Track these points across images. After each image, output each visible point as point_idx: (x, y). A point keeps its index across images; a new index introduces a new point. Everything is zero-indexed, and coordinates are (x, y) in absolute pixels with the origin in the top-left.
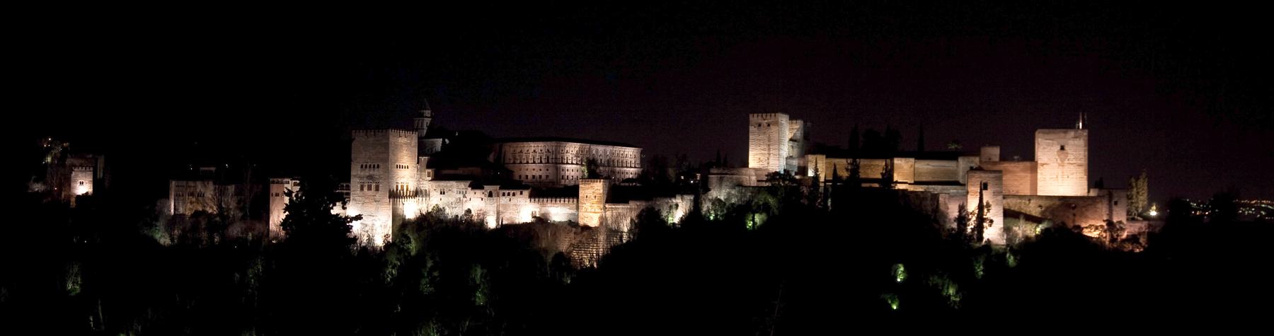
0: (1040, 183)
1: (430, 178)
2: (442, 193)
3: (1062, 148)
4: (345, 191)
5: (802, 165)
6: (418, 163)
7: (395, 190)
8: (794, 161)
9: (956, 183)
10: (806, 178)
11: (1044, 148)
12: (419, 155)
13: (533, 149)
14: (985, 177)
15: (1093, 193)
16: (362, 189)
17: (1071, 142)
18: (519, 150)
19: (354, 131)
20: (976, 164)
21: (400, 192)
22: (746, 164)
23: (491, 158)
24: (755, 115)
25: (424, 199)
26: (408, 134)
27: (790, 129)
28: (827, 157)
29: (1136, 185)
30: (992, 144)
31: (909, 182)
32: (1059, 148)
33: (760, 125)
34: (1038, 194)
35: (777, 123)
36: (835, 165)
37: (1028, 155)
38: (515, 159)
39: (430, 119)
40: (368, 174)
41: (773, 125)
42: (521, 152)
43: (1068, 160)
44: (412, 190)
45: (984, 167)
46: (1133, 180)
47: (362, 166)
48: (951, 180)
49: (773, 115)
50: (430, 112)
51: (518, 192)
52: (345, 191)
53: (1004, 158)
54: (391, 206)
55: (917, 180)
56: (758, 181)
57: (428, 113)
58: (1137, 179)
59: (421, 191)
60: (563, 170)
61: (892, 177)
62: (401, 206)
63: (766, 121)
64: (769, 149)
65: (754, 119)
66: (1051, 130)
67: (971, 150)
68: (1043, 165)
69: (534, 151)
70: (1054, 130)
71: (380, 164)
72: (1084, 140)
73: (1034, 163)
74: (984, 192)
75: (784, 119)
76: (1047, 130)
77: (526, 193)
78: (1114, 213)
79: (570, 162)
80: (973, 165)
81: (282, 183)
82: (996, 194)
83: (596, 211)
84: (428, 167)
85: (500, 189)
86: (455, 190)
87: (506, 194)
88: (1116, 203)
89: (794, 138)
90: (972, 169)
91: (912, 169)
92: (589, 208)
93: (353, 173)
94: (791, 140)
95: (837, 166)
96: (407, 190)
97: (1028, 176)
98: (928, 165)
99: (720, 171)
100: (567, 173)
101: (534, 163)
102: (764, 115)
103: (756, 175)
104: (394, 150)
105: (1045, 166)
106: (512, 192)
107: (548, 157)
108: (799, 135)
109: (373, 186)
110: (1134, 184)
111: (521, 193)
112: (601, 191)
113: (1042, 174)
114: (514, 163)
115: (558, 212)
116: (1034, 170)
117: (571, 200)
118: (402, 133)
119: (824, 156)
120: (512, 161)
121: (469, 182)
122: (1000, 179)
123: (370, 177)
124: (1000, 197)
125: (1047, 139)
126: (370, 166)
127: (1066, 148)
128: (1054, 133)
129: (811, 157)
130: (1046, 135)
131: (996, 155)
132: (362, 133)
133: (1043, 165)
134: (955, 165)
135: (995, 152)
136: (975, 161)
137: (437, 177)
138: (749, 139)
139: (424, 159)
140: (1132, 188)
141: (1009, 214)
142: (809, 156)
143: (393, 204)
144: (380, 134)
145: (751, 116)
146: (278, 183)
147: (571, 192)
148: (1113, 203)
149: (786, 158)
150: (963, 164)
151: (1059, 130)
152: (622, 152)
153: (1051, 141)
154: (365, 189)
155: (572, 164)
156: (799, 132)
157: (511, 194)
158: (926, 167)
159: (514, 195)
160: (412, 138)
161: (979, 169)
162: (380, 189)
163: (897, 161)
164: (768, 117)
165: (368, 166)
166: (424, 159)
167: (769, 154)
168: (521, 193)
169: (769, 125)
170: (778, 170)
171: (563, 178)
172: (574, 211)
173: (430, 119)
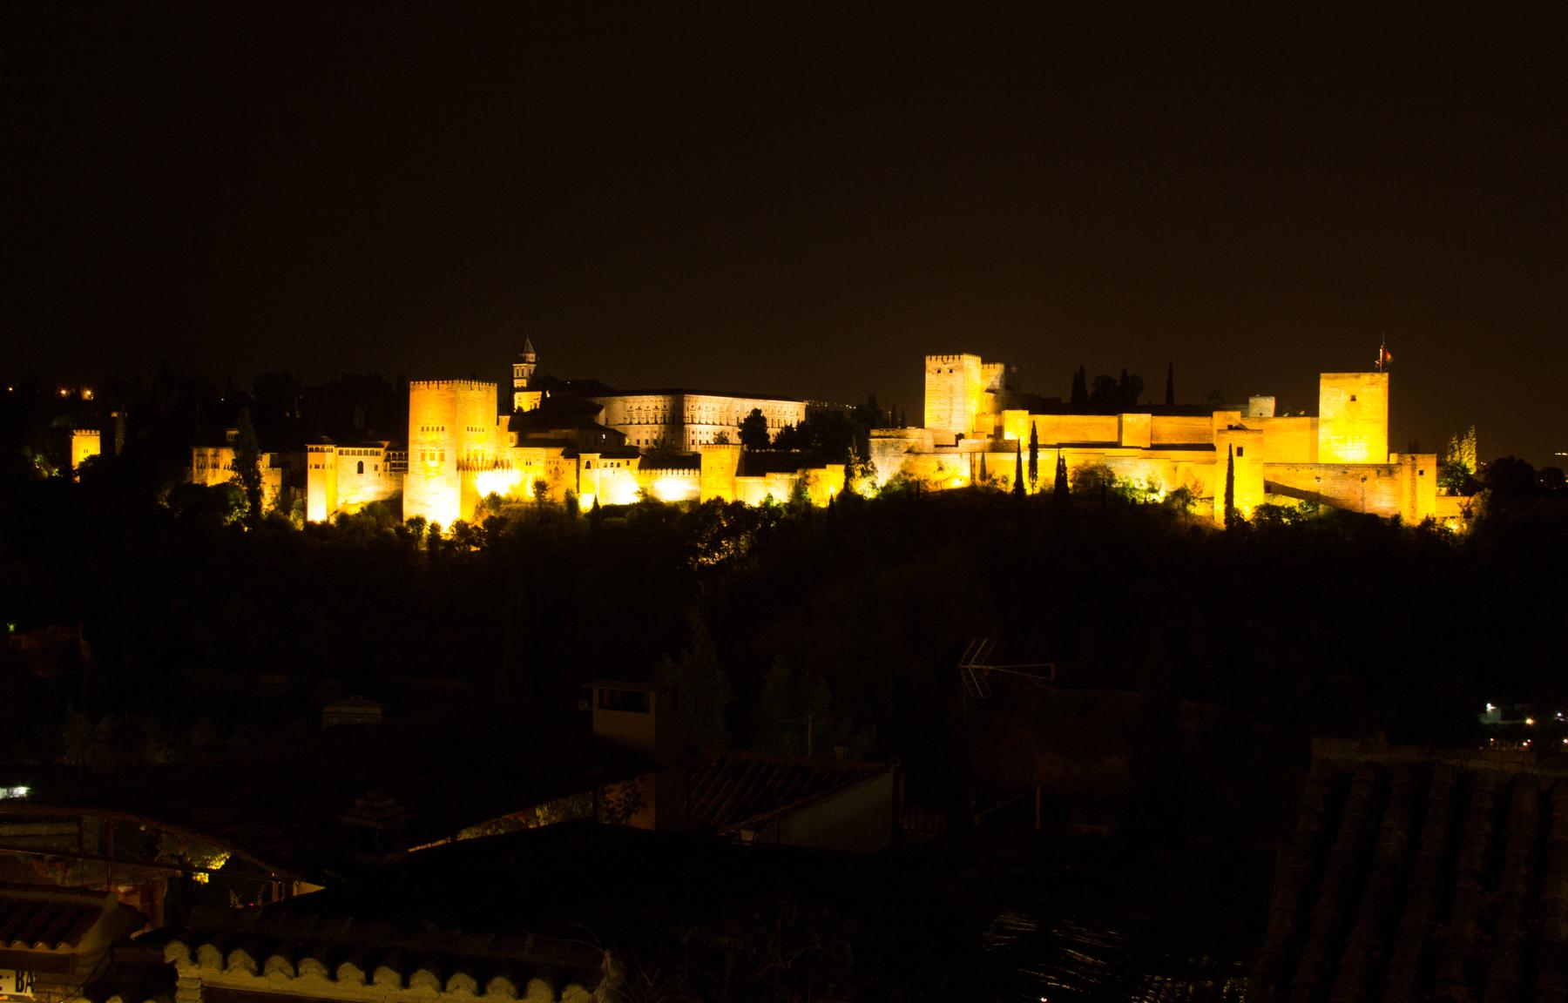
0: (1321, 447)
1: (514, 444)
2: (528, 463)
3: (1353, 399)
4: (404, 462)
5: (997, 425)
6: (498, 424)
7: (465, 460)
8: (987, 419)
9: (1211, 447)
10: (1000, 441)
11: (1328, 399)
12: (498, 415)
13: (652, 406)
14: (1237, 439)
15: (1394, 458)
16: (423, 457)
17: (1365, 390)
18: (636, 406)
19: (412, 383)
20: (1237, 421)
21: (472, 463)
22: (920, 424)
23: (602, 418)
24: (934, 358)
25: (505, 470)
26: (483, 386)
27: (982, 377)
28: (1030, 413)
29: (1460, 449)
30: (1265, 394)
31: (1143, 446)
32: (1348, 398)
33: (939, 372)
34: (1322, 460)
35: (961, 368)
36: (1034, 423)
37: (1309, 406)
38: (632, 418)
39: (534, 365)
40: (430, 439)
41: (956, 370)
42: (639, 408)
43: (1361, 414)
44: (489, 460)
45: (1247, 424)
46: (1455, 441)
47: (423, 430)
48: (1202, 442)
49: (956, 357)
50: (533, 355)
51: (623, 462)
52: (404, 462)
53: (1278, 413)
54: (459, 482)
55: (1154, 442)
56: (936, 446)
57: (531, 357)
58: (1460, 440)
59: (502, 462)
60: (693, 433)
61: (1037, 443)
62: (474, 481)
63: (947, 366)
64: (952, 403)
65: (932, 363)
66: (1338, 375)
67: (1239, 401)
68: (1326, 421)
69: (656, 408)
70: (1342, 374)
71: (445, 426)
72: (1383, 387)
73: (1315, 419)
74: (1236, 459)
75: (971, 363)
76: (1332, 375)
77: (635, 462)
78: (1419, 487)
79: (703, 421)
80: (1231, 423)
81: (323, 451)
82: (1254, 461)
83: (724, 487)
84: (511, 428)
85: (601, 457)
86: (543, 459)
87: (609, 465)
88: (1421, 473)
89: (993, 388)
90: (1230, 428)
91: (1149, 429)
92: (715, 483)
93: (412, 437)
94: (988, 391)
95: (1036, 424)
96: (483, 460)
97: (1307, 434)
98: (1170, 422)
99: (882, 434)
100: (699, 437)
101: (656, 423)
102: (945, 357)
103: (934, 438)
104: (463, 408)
105: (1328, 423)
106: (615, 461)
107: (674, 416)
108: (997, 384)
109: (437, 454)
110: (1456, 446)
111: (628, 464)
112: (730, 461)
113: (1324, 432)
114: (631, 423)
115: (673, 487)
116: (1315, 427)
117: (692, 471)
118: (475, 385)
119: (1027, 412)
120: (628, 422)
121: (562, 449)
122: (1260, 441)
123: (434, 443)
124: (1259, 467)
125: (1332, 387)
126: (433, 430)
127: (1357, 398)
128: (1341, 378)
129: (1008, 413)
130: (1331, 381)
131: (1268, 409)
132: (422, 385)
133: (1326, 421)
134: (1208, 423)
135: (1267, 404)
136: (1235, 417)
137: (523, 442)
138: (924, 390)
139: (506, 419)
140: (1455, 451)
141: (1269, 488)
142: (1006, 411)
143: (463, 479)
144: (445, 386)
145: (928, 358)
146: (317, 450)
147: (693, 462)
148: (1418, 472)
149: (977, 416)
150: (1220, 419)
151: (1347, 375)
152: (778, 408)
153: (1337, 390)
154: (427, 458)
155: (707, 424)
156: (998, 380)
157: (615, 465)
158: (1169, 425)
159: (618, 465)
160: (489, 392)
161: (1239, 428)
162: (446, 458)
163: (1128, 418)
164: (951, 360)
165: (430, 429)
166: (506, 419)
167: (952, 410)
168: (628, 464)
169: (951, 371)
170: (962, 432)
171: (693, 444)
172: (696, 487)
173: (534, 365)
